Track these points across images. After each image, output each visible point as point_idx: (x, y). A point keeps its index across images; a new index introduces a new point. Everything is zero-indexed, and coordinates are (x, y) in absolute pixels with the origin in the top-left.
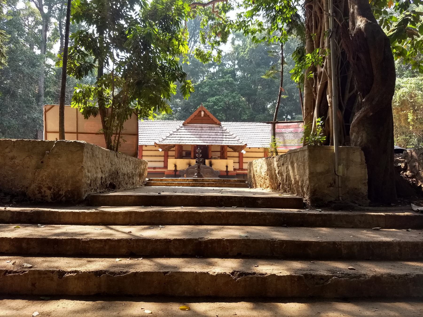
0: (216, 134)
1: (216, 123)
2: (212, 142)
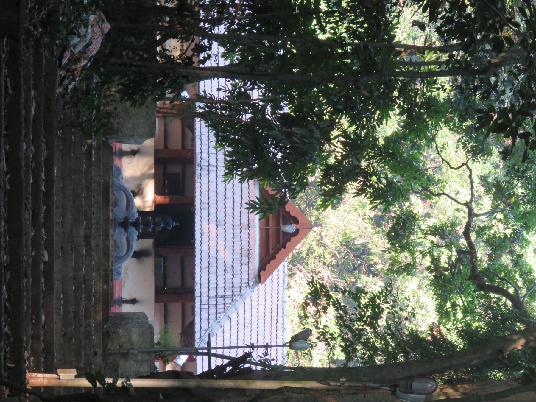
0: (229, 269)
1: (262, 267)
2: (205, 256)
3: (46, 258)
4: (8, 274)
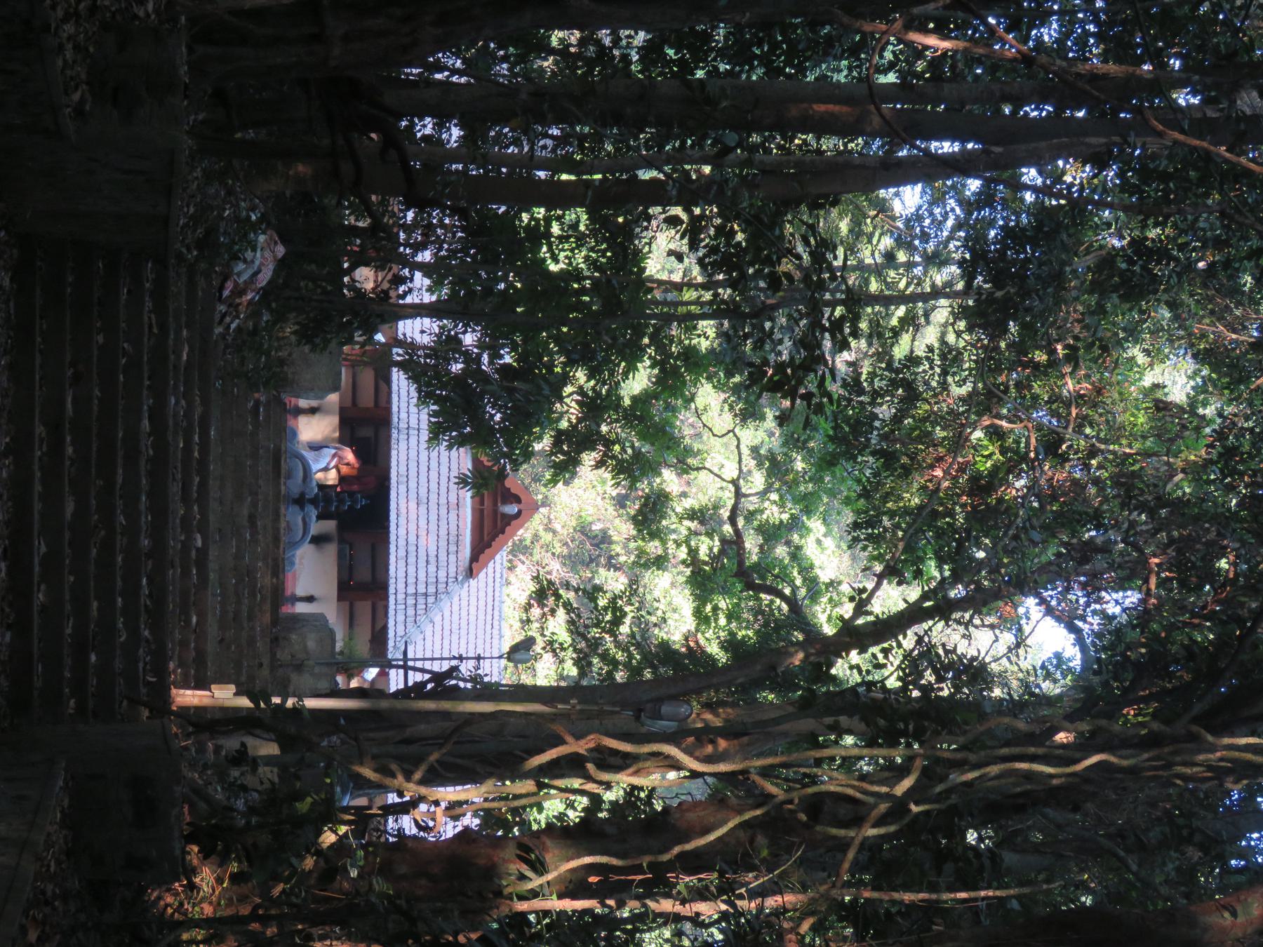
0: (432, 560)
1: (475, 558)
2: (402, 542)
3: (199, 543)
4: (150, 562)
